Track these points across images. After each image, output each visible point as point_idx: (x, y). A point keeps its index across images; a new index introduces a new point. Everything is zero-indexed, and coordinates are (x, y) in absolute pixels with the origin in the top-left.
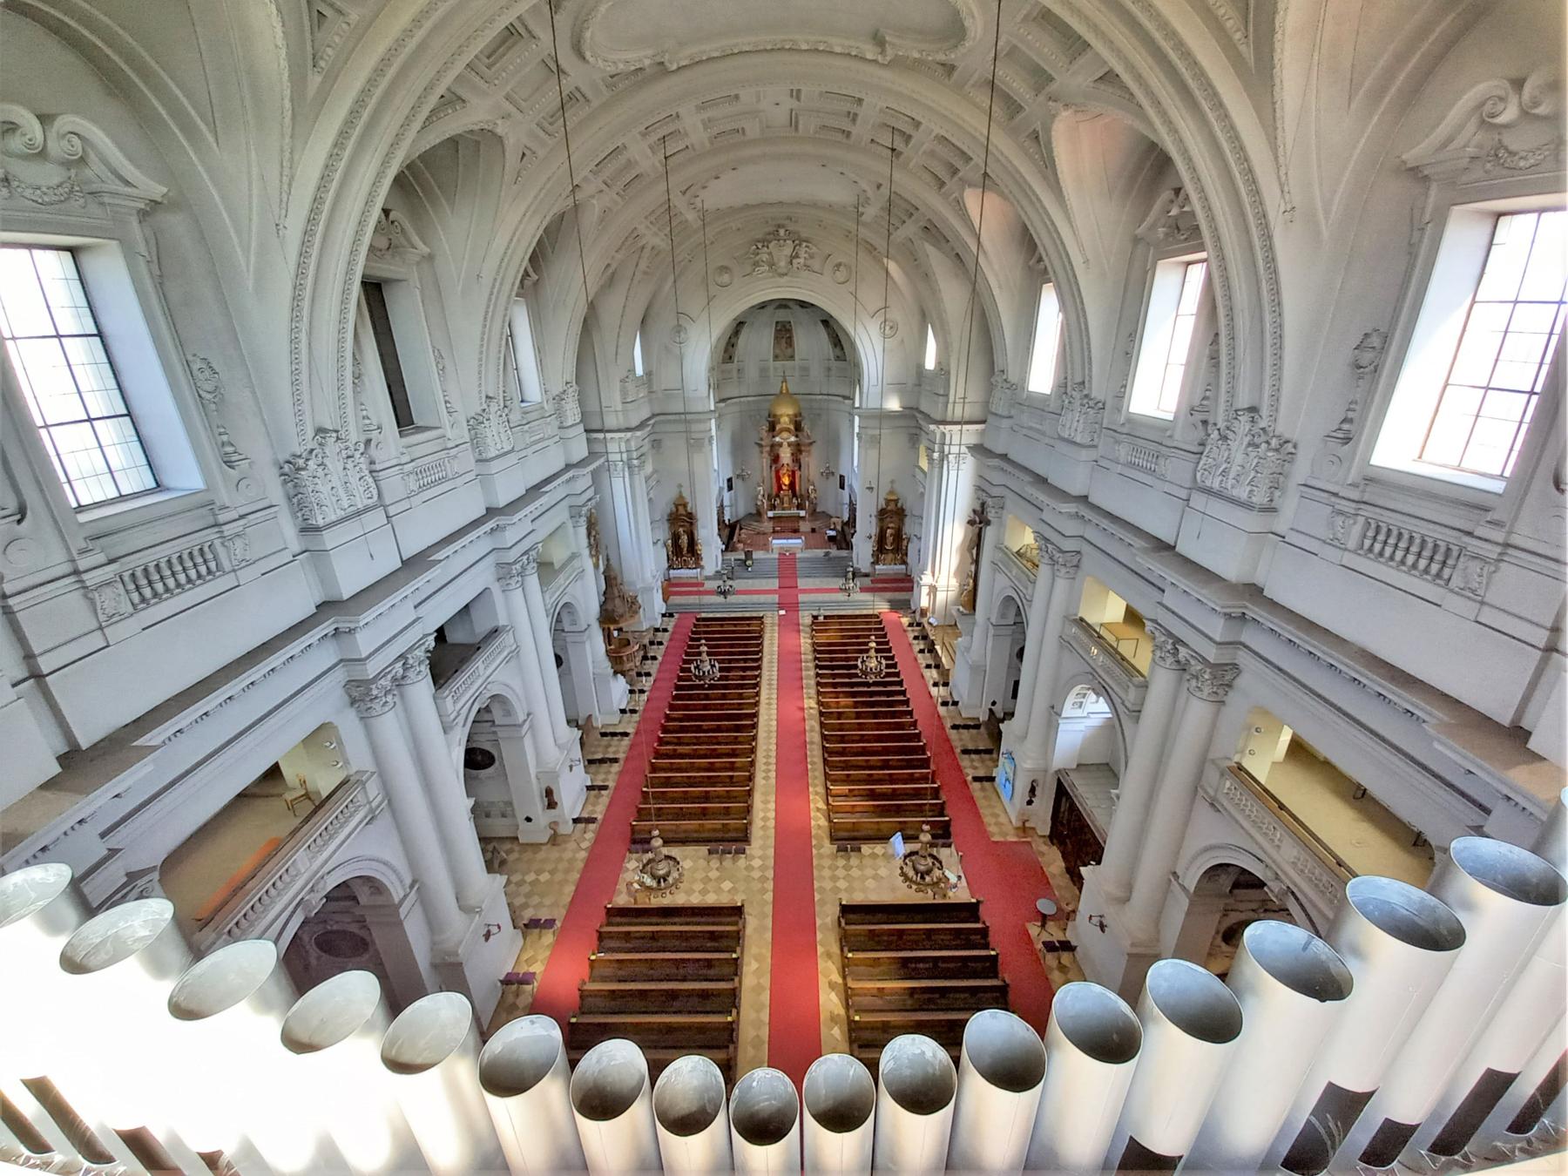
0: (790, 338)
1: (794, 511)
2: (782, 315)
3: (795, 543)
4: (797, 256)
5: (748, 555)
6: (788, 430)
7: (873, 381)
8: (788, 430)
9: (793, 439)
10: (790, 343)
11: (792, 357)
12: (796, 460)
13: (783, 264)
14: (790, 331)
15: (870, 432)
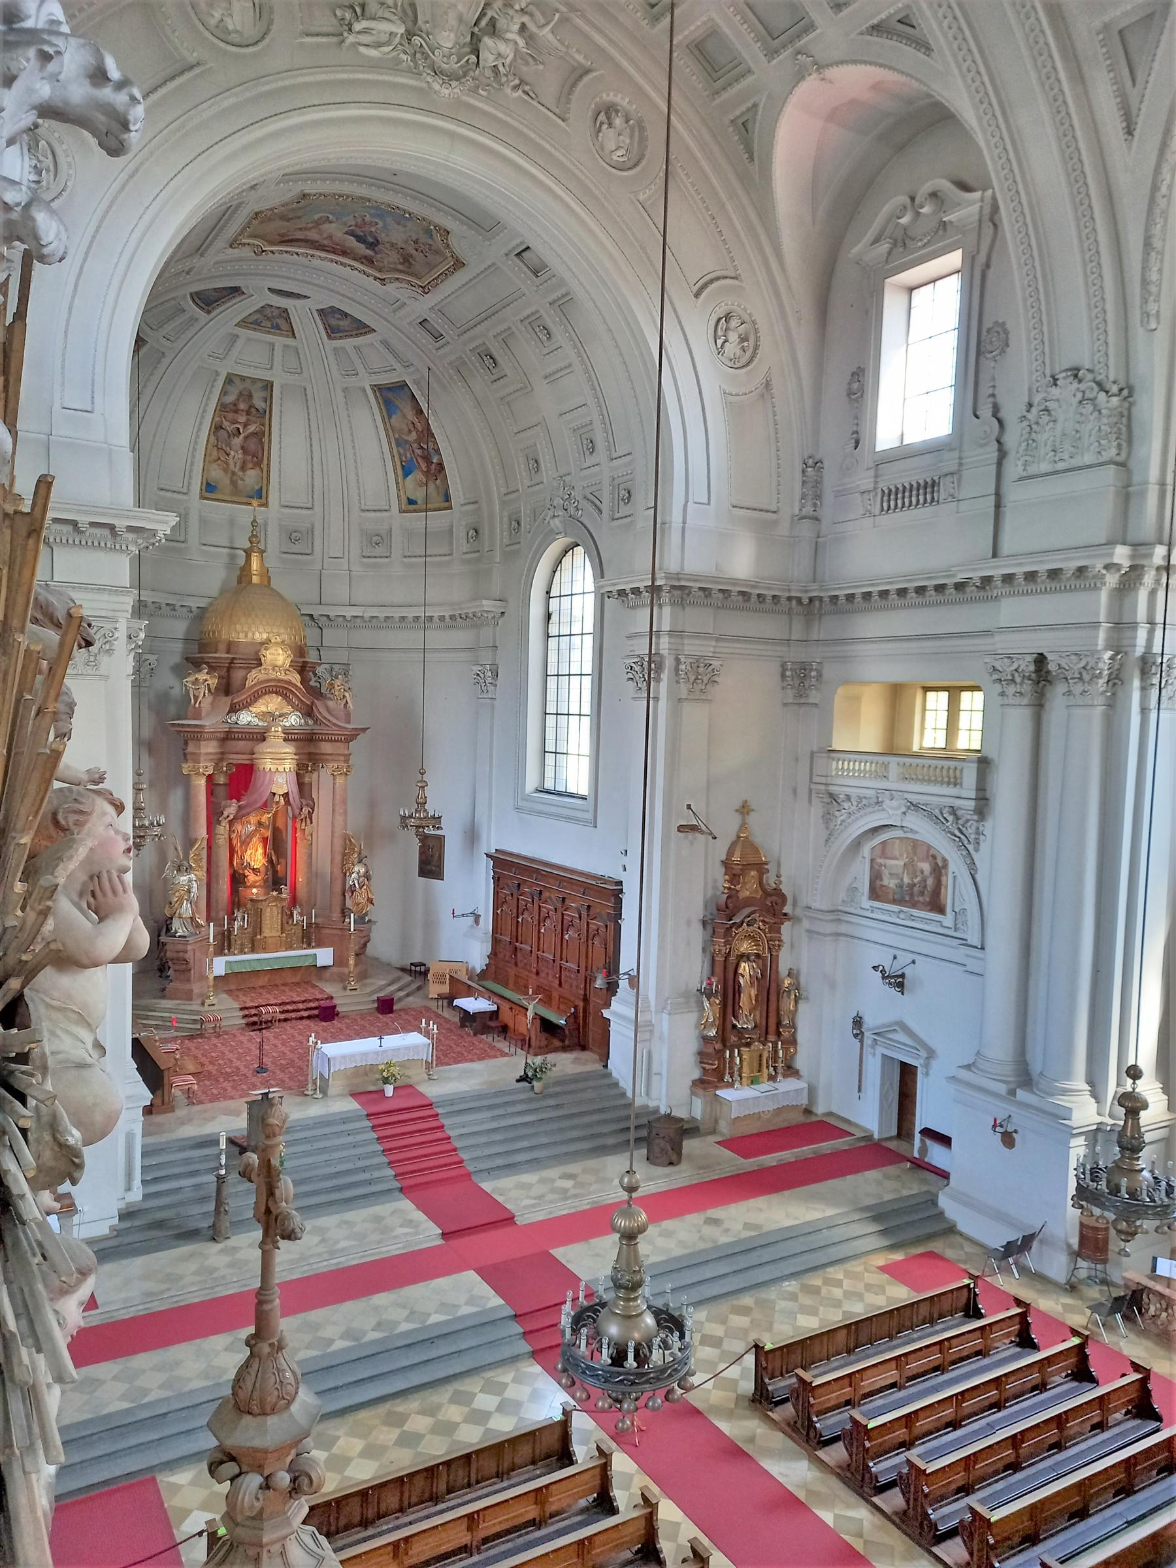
0: (259, 435)
1: (298, 954)
2: (253, 356)
3: (408, 1044)
4: (493, 29)
5: (260, 1111)
6: (281, 689)
7: (699, 493)
8: (281, 689)
9: (294, 720)
10: (257, 453)
11: (260, 495)
12: (303, 787)
13: (447, 39)
14: (264, 415)
15: (692, 648)
